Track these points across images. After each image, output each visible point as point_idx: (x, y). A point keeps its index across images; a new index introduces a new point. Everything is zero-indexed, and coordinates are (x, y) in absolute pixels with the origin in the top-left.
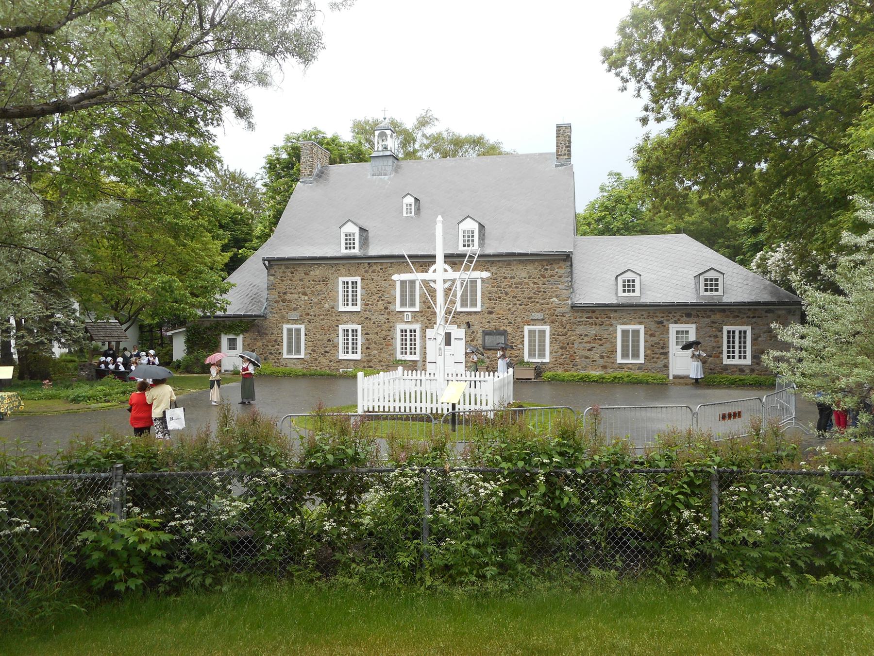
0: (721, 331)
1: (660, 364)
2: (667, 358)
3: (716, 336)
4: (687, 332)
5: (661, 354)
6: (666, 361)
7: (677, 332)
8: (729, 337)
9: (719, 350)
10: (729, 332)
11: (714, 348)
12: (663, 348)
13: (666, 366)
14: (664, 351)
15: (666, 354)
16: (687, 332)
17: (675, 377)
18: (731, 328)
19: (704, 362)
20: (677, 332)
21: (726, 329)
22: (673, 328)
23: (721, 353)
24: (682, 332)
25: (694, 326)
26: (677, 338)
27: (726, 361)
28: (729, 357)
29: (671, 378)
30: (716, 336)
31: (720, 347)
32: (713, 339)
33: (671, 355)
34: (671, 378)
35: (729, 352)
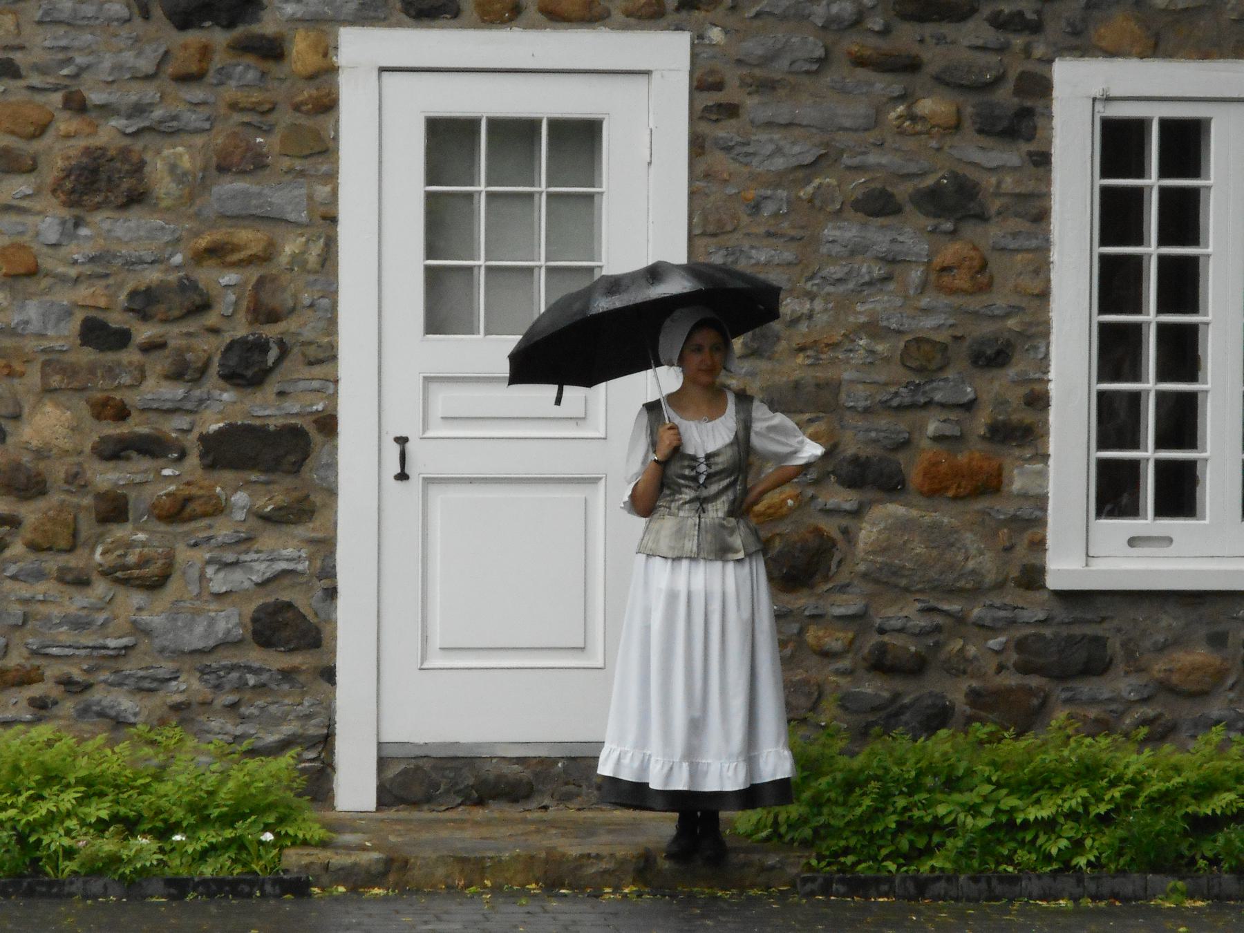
0: (1020, 120)
1: (209, 600)
2: (308, 509)
3: (955, 202)
4: (579, 139)
5: (234, 450)
6: (287, 549)
7: (448, 139)
8: (1118, 216)
9: (998, 387)
10: (1120, 143)
11: (925, 357)
12: (248, 366)
13: (294, 631)
14: (264, 408)
15: (289, 457)
16: (579, 139)
17: (415, 780)
18: (1152, 85)
19: (796, 569)
20: (448, 139)
21: (1083, 91)
22: (389, 94)
23: (1023, 431)
24: (515, 134)
25: (668, 52)
26: (442, 222)
27: (1088, 552)
28: (1114, 492)
29: (355, 788)
30: (955, 202)
31: (1011, 348)
32: (911, 236)
33: (356, 459)
34: (355, 788)
35: (1115, 421)
